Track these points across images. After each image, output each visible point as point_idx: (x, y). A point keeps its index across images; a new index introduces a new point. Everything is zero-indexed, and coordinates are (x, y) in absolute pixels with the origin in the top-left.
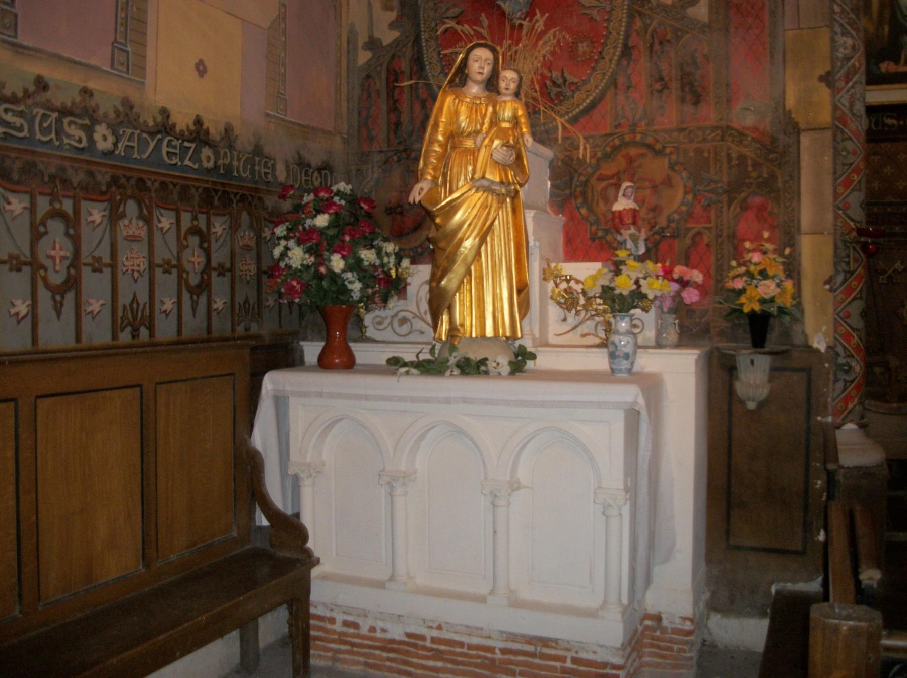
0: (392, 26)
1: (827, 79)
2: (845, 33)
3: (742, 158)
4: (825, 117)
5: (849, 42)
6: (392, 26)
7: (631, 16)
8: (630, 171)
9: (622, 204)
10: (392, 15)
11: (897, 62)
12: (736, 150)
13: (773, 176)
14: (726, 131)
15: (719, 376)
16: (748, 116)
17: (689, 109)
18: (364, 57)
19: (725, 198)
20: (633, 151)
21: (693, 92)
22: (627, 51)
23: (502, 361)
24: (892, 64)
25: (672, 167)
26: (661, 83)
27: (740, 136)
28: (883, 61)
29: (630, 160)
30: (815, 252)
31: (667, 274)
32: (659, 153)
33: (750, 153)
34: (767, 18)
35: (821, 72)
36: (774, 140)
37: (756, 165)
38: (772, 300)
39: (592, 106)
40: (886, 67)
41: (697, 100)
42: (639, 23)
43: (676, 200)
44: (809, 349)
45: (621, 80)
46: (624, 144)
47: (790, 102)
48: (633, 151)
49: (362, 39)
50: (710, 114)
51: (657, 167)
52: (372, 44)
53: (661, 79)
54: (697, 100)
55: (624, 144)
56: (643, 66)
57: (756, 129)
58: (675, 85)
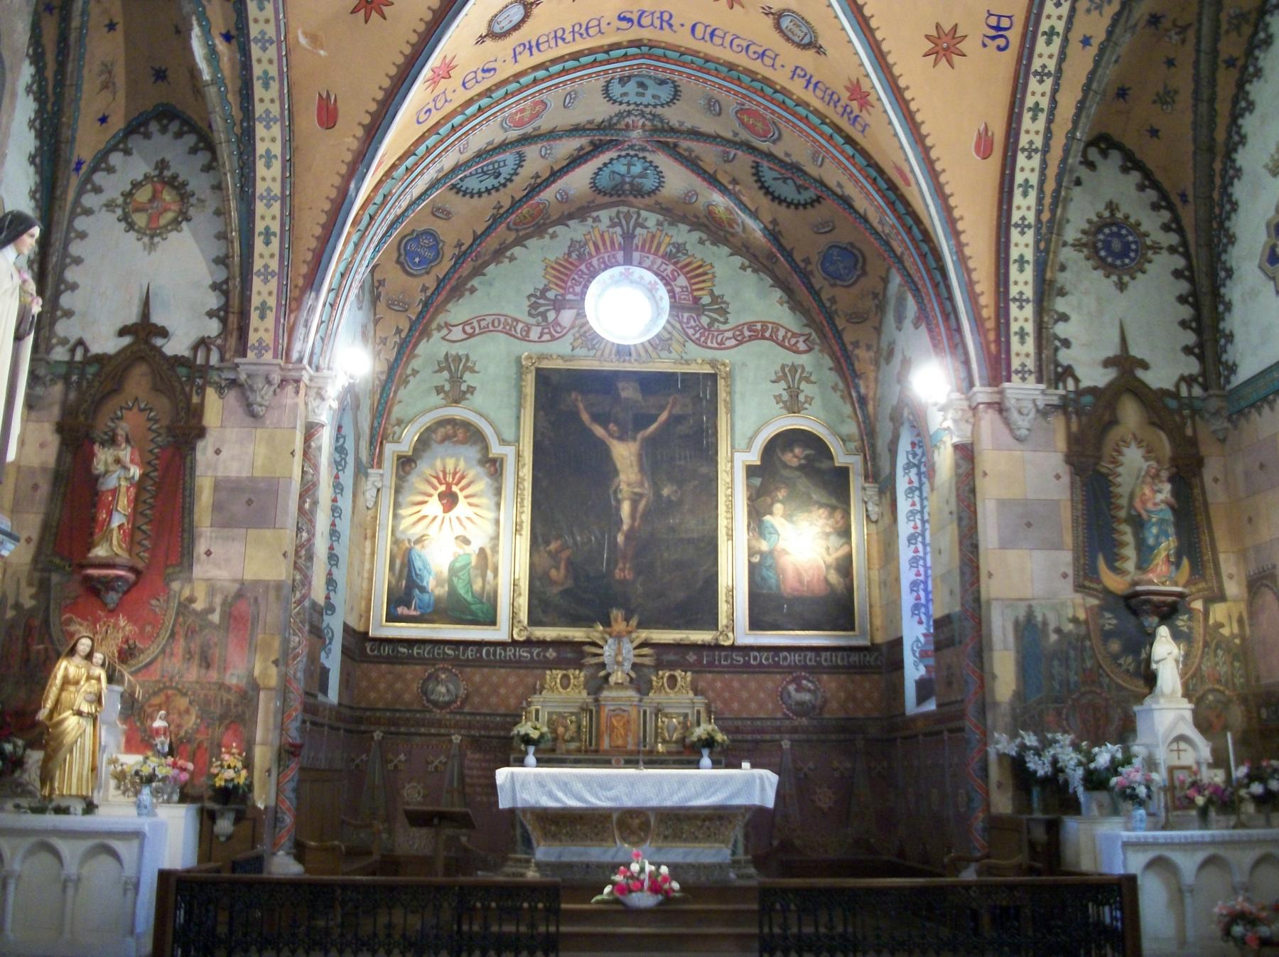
0: (32, 597)
1: (276, 663)
2: (295, 634)
3: (229, 701)
4: (273, 681)
5: (297, 639)
6: (32, 597)
7: (177, 614)
8: (167, 704)
9: (159, 723)
10: (33, 590)
11: (409, 607)
12: (226, 696)
13: (244, 713)
14: (221, 686)
15: (207, 819)
16: (234, 678)
17: (203, 671)
18: (10, 614)
19: (217, 723)
20: (170, 692)
21: (206, 663)
22: (173, 635)
23: (79, 807)
25: (191, 703)
26: (189, 656)
27: (229, 689)
28: (399, 605)
29: (168, 697)
30: (262, 755)
31: (174, 765)
32: (185, 694)
33: (233, 698)
34: (249, 625)
35: (273, 658)
36: (246, 693)
37: (236, 706)
38: (232, 780)
39: (150, 663)
40: (401, 610)
41: (208, 666)
42: (181, 619)
43: (191, 721)
44: (255, 807)
45: (168, 650)
46: (165, 687)
47: (256, 673)
48: (170, 692)
49: (11, 601)
50: (214, 675)
51: (183, 703)
52: (17, 606)
53: (190, 652)
54: (208, 666)
55: (165, 687)
56: (181, 644)
57: (237, 686)
58: (197, 657)
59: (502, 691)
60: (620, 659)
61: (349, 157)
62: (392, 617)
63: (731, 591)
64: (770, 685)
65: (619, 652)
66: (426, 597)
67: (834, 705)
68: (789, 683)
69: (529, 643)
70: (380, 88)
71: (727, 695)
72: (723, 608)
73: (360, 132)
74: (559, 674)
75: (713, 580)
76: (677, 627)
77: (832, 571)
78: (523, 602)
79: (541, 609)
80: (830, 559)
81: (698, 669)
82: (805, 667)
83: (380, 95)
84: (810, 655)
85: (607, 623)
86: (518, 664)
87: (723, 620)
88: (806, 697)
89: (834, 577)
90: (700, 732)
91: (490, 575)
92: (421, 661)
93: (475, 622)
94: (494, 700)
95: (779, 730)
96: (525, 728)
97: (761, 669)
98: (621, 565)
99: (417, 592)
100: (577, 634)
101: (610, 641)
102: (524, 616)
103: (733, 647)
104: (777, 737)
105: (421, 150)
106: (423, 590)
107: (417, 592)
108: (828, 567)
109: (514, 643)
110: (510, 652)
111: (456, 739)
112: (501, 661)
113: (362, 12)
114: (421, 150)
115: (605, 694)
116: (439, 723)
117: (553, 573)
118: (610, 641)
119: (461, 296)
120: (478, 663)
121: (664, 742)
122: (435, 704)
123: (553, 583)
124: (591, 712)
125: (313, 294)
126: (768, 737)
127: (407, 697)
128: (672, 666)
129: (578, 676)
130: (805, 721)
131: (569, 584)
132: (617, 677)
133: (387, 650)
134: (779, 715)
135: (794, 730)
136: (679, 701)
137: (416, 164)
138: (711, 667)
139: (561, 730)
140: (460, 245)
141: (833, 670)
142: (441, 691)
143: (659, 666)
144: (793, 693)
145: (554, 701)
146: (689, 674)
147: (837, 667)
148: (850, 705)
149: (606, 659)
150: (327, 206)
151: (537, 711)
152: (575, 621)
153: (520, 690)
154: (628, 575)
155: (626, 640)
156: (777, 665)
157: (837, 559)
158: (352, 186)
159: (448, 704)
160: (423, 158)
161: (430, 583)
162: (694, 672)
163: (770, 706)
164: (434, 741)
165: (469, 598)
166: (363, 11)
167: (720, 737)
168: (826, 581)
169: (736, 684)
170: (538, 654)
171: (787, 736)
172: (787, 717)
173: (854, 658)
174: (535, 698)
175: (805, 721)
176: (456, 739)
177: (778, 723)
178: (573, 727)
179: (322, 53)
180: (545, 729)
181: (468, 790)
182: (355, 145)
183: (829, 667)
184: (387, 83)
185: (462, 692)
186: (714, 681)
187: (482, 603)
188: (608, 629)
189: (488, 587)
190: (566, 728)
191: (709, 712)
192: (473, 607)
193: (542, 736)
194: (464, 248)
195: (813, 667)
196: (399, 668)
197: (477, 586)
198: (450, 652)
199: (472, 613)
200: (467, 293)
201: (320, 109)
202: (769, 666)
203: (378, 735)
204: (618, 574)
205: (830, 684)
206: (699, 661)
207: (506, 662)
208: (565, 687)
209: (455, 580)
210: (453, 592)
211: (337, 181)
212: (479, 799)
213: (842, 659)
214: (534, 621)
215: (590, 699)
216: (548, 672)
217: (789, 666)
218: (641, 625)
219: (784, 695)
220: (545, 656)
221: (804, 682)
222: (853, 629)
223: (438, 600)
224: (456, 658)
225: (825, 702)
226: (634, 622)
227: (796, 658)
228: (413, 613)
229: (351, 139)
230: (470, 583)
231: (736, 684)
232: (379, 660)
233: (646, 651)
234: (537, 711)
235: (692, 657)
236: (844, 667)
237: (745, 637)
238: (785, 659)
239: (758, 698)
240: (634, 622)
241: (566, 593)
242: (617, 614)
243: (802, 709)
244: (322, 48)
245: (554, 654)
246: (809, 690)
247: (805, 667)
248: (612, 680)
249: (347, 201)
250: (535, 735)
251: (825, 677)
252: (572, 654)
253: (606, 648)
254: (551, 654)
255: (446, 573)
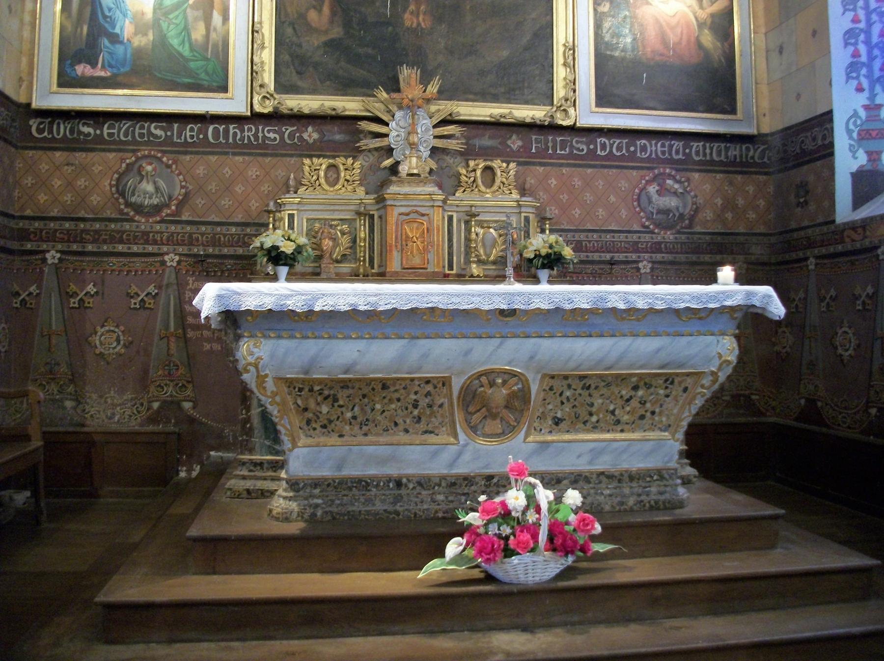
11: (94, 65)
24: (89, 67)
28: (80, 62)
40: (82, 69)
59: (239, 189)
60: (414, 139)
62: (66, 81)
63: (572, 49)
64: (624, 184)
65: (412, 131)
66: (120, 49)
67: (708, 214)
68: (649, 182)
69: (276, 117)
71: (564, 197)
72: (560, 73)
74: (324, 163)
75: (546, 32)
76: (495, 98)
77: (706, 31)
78: (267, 56)
79: (294, 66)
80: (703, 15)
81: (525, 159)
82: (670, 162)
84: (677, 144)
85: (394, 86)
86: (262, 149)
87: (560, 91)
88: (671, 202)
89: (708, 39)
90: (539, 243)
91: (217, 19)
92: (118, 146)
93: (196, 87)
94: (225, 202)
95: (635, 247)
96: (271, 238)
97: (610, 162)
98: (412, 7)
99: (105, 42)
100: (350, 105)
101: (399, 114)
102: (268, 77)
103: (572, 129)
104: (634, 257)
106: (115, 39)
107: (105, 42)
108: (701, 25)
109: (256, 117)
110: (249, 132)
111: (171, 259)
112: (235, 145)
115: (393, 189)
116: (146, 237)
117: (312, 15)
118: (399, 114)
120: (202, 147)
121: (480, 262)
122: (139, 209)
123: (311, 29)
124: (372, 217)
126: (621, 257)
127: (95, 199)
128: (487, 153)
129: (352, 167)
130: (669, 236)
131: (337, 32)
132: (410, 165)
133: (62, 129)
134: (636, 227)
135: (656, 248)
136: (498, 200)
138: (542, 157)
139: (327, 244)
141: (708, 166)
142: (146, 190)
143: (467, 154)
144: (655, 197)
145: (317, 199)
146: (512, 165)
147: (712, 162)
148: (729, 215)
149: (391, 140)
151: (291, 217)
152: (346, 87)
153: (265, 188)
154: (424, 21)
155: (420, 113)
156: (632, 156)
157: (712, 15)
159: (157, 209)
161: (126, 28)
162: (519, 164)
163: (624, 213)
164: (138, 263)
165: (186, 51)
167: (568, 252)
168: (700, 45)
169: (577, 182)
170: (292, 136)
171: (647, 256)
172: (647, 230)
173: (735, 151)
174: (290, 199)
175: (669, 236)
176: (171, 259)
177: (635, 237)
178: (345, 241)
180: (303, 240)
181: (190, 334)
183: (700, 163)
185: (178, 192)
186: (547, 177)
187: (207, 59)
188: (395, 95)
189: (213, 36)
190: (334, 239)
191: (542, 220)
192: (192, 65)
193: (299, 250)
195: (679, 162)
196: (80, 156)
197: (198, 33)
198: (158, 132)
199: (190, 73)
202: (622, 158)
203: (53, 257)
204: (409, 20)
205: (703, 186)
206: (526, 148)
207: (244, 146)
208: (333, 184)
209: (164, 25)
210: (162, 41)
212: (207, 347)
213: (719, 153)
214: (283, 86)
215: (370, 199)
216: (307, 161)
217: (649, 159)
218: (445, 94)
219: (641, 197)
220: (301, 138)
221: (669, 182)
222: (733, 111)
223: (138, 53)
224: (168, 142)
225: (697, 211)
226: (433, 88)
227: (656, 148)
228: (100, 73)
230: (186, 29)
231: (577, 182)
232: (50, 145)
233: (450, 129)
234: (291, 217)
235: (515, 143)
236: (721, 163)
237: (588, 114)
238: (644, 149)
239: (611, 200)
240: (433, 88)
241: (332, 45)
242: (407, 74)
243: (666, 219)
245: (315, 136)
246: (675, 193)
247: (670, 162)
248: (404, 169)
250: (288, 248)
251: (696, 175)
252: (344, 134)
253: (393, 124)
254: (311, 134)
255: (149, 14)
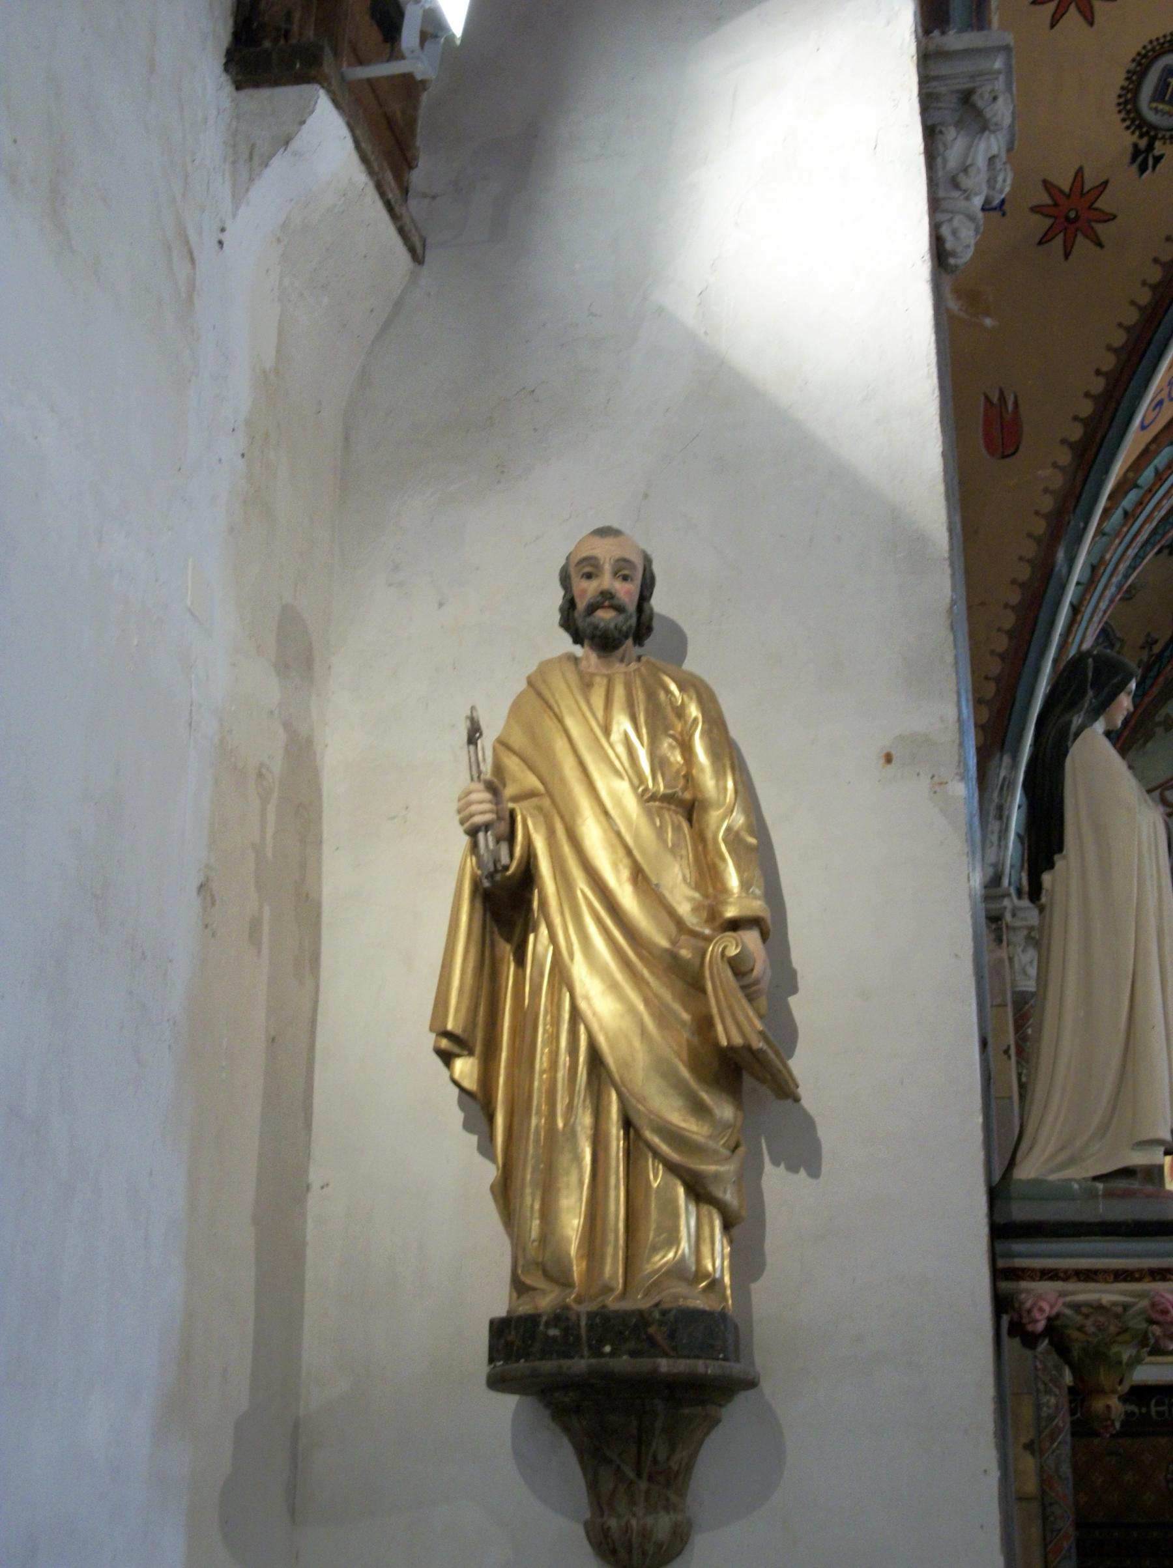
2: (1048, 1392)
5: (1053, 1400)
35: (1024, 1440)
61: (1047, 504)
70: (1098, 372)
73: (1065, 457)
83: (1098, 385)
105: (1148, 475)
113: (1059, 241)
114: (1148, 475)
119: (1149, 736)
125: (1007, 759)
137: (1141, 504)
140: (1150, 643)
150: (1015, 598)
158: (1061, 555)
160: (1151, 491)
166: (1059, 240)
179: (988, 322)
182: (1058, 481)
184: (1109, 362)
194: (1157, 649)
200: (1159, 731)
201: (987, 423)
211: (1030, 550)
229: (1049, 472)
244: (987, 314)
249: (1053, 583)
